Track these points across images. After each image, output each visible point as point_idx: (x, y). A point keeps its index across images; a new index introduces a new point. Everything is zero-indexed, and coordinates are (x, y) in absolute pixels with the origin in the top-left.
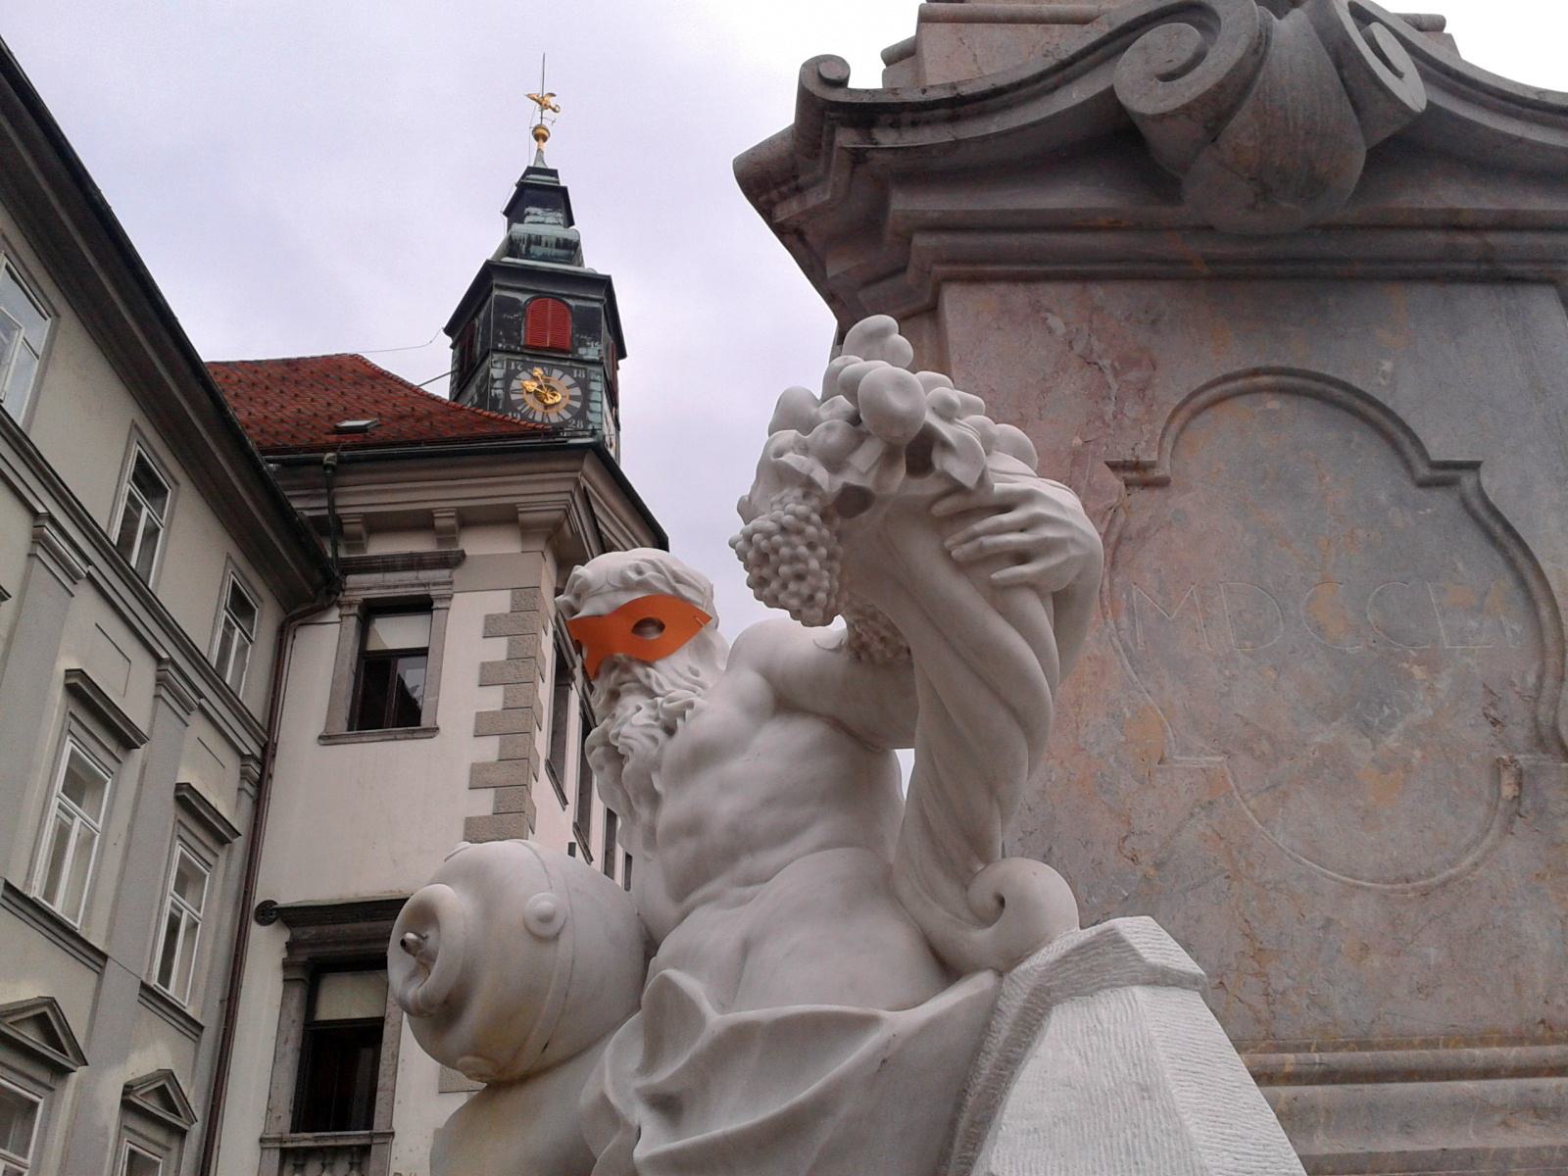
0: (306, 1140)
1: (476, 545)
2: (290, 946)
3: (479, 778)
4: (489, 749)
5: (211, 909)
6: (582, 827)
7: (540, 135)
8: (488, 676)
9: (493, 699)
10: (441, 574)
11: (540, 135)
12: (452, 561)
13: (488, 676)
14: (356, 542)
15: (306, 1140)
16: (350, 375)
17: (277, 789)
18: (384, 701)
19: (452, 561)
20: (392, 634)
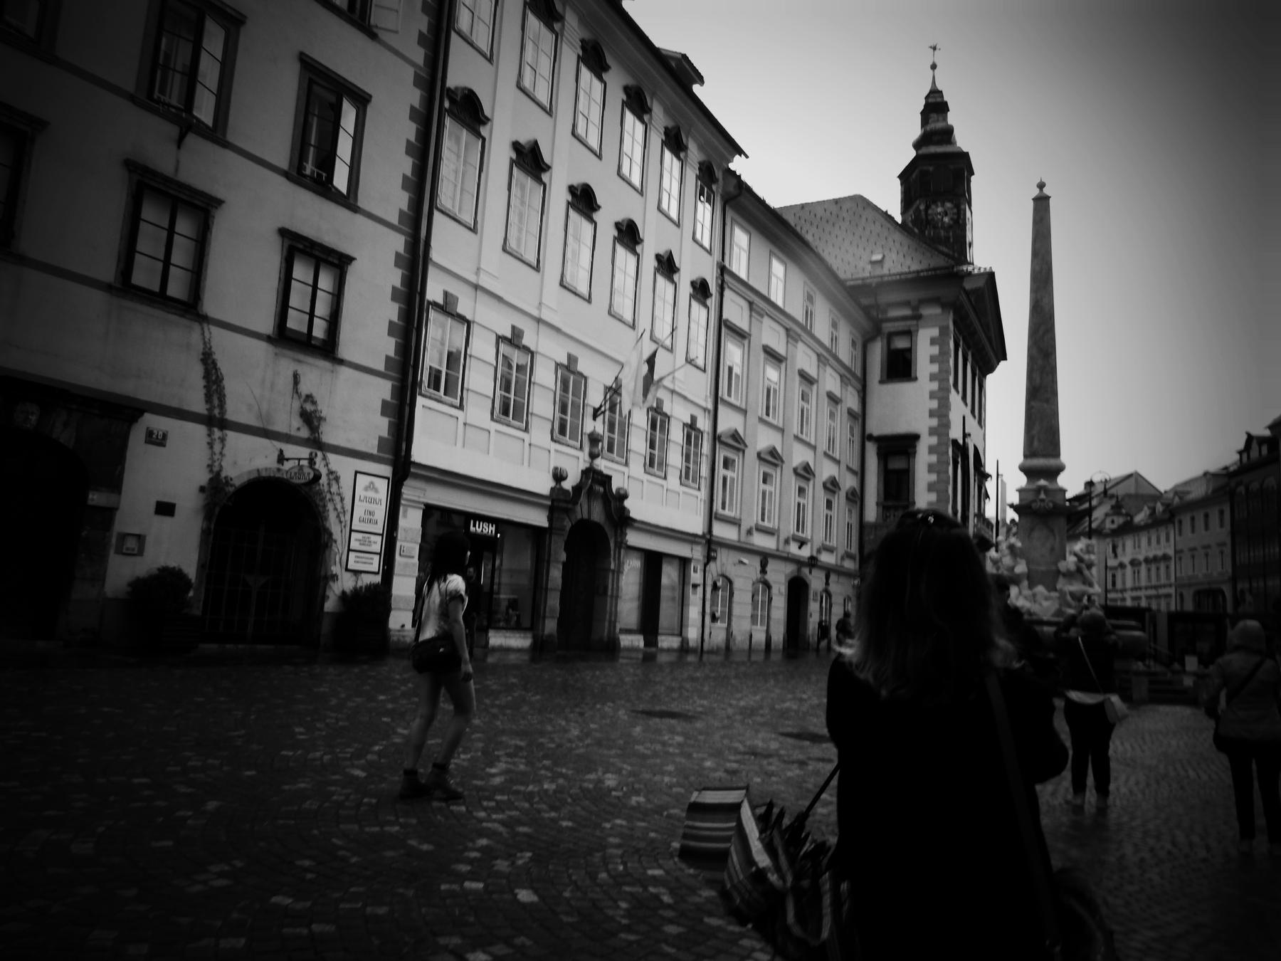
0: (890, 503)
1: (927, 311)
2: (879, 449)
3: (932, 395)
4: (935, 386)
5: (857, 438)
6: (964, 398)
7: (934, 67)
8: (933, 360)
9: (935, 368)
10: (914, 322)
11: (934, 67)
12: (918, 317)
13: (933, 360)
14: (885, 312)
15: (890, 503)
16: (860, 203)
17: (868, 400)
18: (900, 367)
19: (918, 317)
20: (901, 343)
